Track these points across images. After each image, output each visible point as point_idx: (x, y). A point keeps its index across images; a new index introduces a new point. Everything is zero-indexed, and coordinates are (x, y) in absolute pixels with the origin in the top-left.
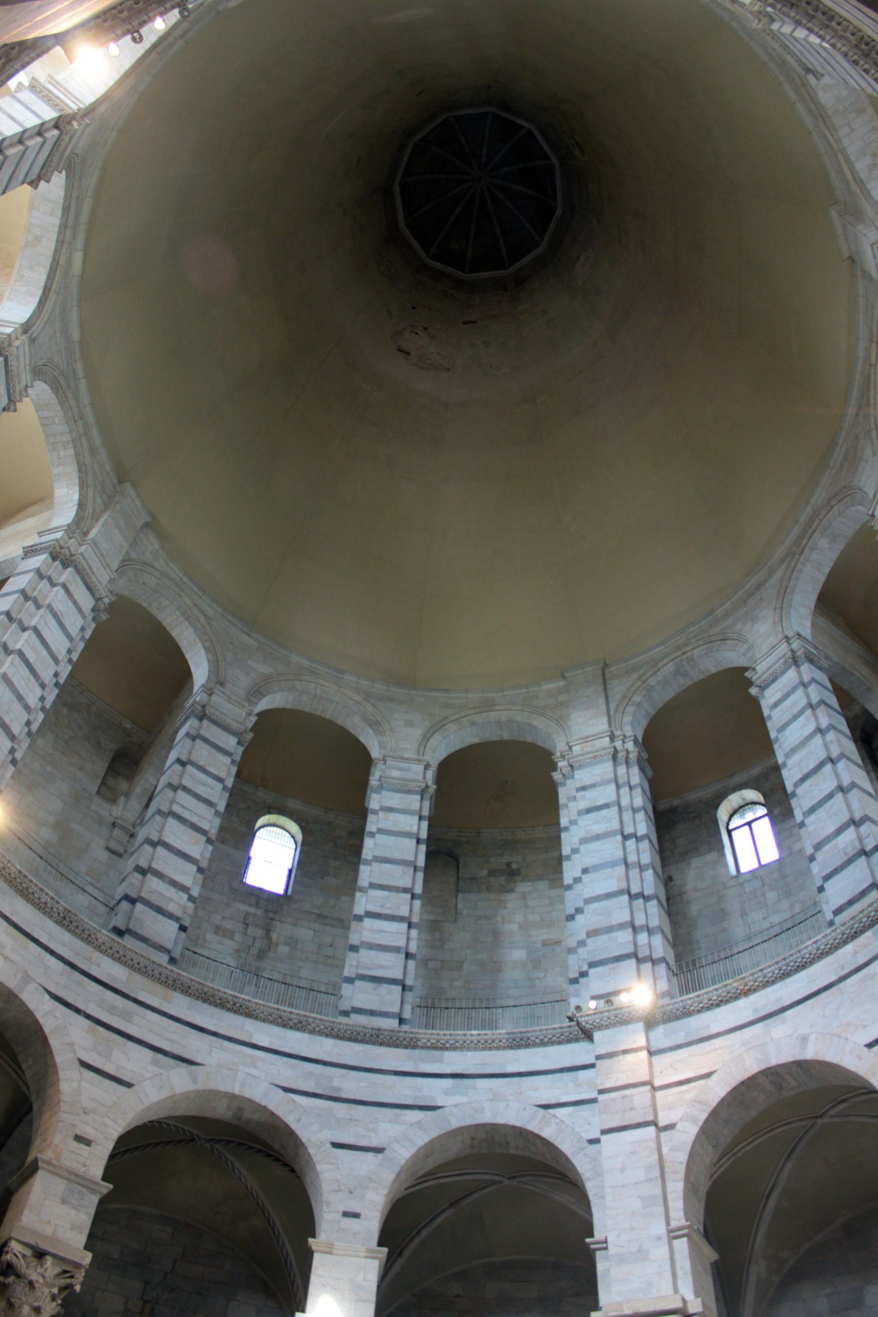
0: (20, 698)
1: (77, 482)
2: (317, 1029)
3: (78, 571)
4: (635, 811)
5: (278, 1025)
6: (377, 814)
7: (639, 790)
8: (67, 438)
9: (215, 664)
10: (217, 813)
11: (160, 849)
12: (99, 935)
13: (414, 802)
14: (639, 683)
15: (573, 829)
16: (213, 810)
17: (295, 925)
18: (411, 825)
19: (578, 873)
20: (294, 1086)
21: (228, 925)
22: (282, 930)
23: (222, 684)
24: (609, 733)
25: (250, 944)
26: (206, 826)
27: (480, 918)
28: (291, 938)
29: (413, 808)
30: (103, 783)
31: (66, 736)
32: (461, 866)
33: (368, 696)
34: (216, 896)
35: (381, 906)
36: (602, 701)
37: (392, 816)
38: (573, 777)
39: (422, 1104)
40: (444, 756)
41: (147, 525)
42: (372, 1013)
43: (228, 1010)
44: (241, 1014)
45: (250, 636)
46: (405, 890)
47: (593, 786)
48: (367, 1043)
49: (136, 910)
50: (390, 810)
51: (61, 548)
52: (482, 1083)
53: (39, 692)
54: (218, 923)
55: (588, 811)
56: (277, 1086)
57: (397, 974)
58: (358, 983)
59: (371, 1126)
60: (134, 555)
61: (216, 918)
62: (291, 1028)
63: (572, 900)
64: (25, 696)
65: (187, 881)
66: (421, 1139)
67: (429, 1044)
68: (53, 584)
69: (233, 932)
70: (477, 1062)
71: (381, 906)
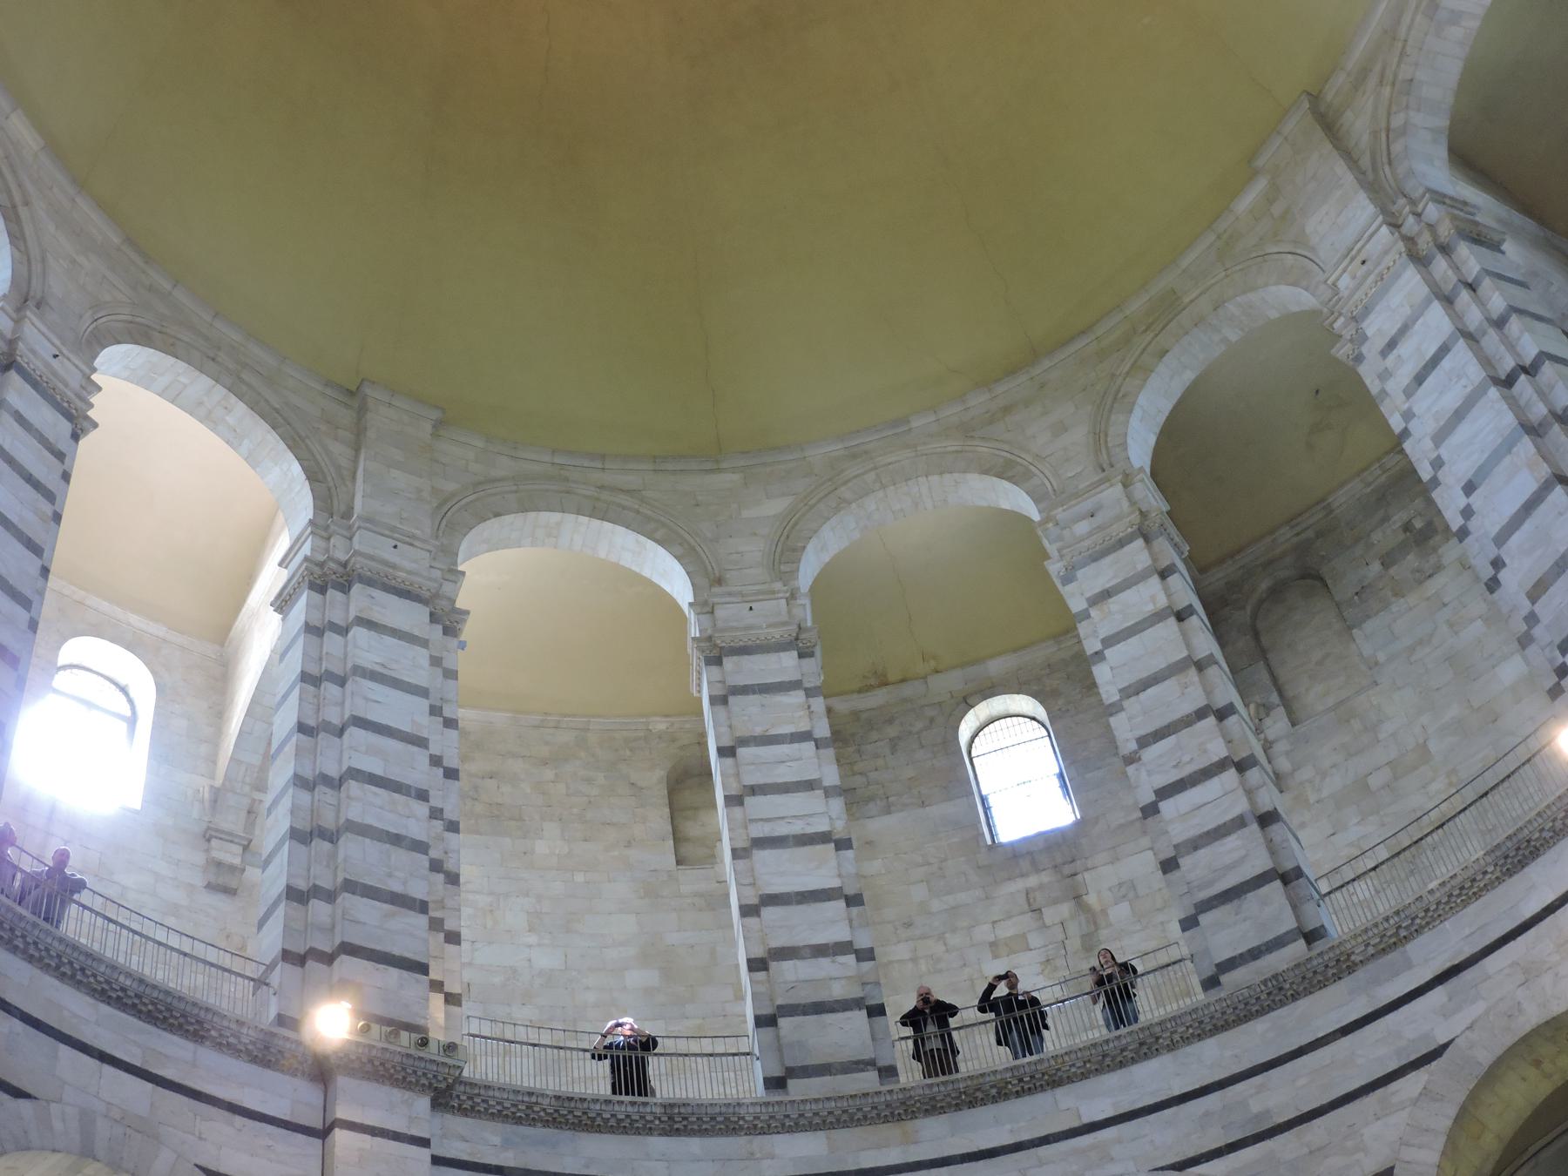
0: (396, 840)
1: (282, 446)
2: (1176, 1037)
3: (370, 582)
4: (1500, 323)
5: (1110, 1069)
6: (1089, 616)
7: (1487, 283)
8: (220, 391)
9: (689, 557)
10: (829, 792)
11: (769, 913)
12: (742, 1111)
13: (1137, 555)
14: (1387, 91)
15: (1413, 426)
16: (820, 792)
17: (1115, 860)
18: (1153, 599)
19: (1462, 501)
20: (1191, 1154)
21: (1007, 931)
22: (1099, 883)
23: (719, 581)
24: (1381, 218)
25: (1061, 936)
26: (822, 826)
27: (1412, 649)
28: (1120, 885)
29: (1140, 567)
30: (678, 838)
31: (575, 811)
32: (1329, 582)
33: (967, 430)
34: (963, 897)
35: (1175, 767)
36: (1341, 167)
37: (1114, 604)
38: (1364, 338)
39: (1413, 1057)
40: (1152, 440)
41: (438, 425)
42: (1254, 954)
43: (1018, 1094)
44: (1042, 1089)
45: (719, 470)
46: (1201, 714)
47: (1404, 330)
48: (1271, 1009)
49: (783, 1032)
50: (1106, 594)
51: (321, 565)
52: (1492, 962)
53: (421, 809)
54: (992, 938)
55: (1420, 379)
56: (1162, 1169)
57: (1261, 862)
58: (1204, 919)
59: (1349, 1144)
60: (451, 487)
61: (984, 933)
62: (1134, 1061)
63: (1478, 551)
64: (403, 832)
65: (840, 934)
66: (1442, 1118)
67: (1371, 950)
68: (343, 631)
69: (1024, 936)
70: (1467, 931)
71: (1175, 767)
